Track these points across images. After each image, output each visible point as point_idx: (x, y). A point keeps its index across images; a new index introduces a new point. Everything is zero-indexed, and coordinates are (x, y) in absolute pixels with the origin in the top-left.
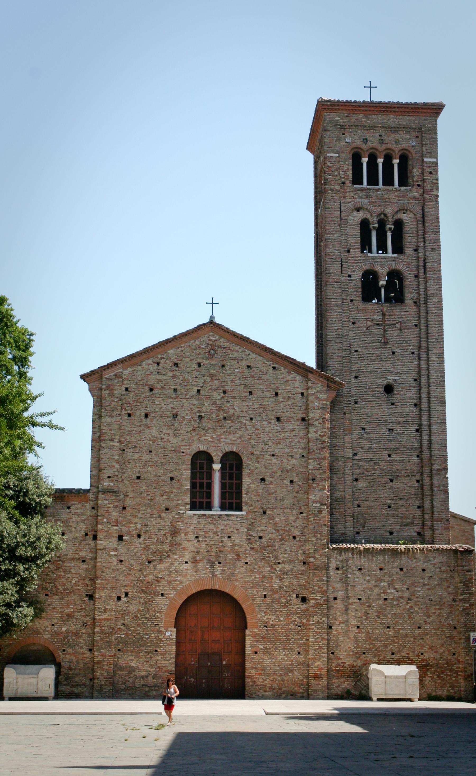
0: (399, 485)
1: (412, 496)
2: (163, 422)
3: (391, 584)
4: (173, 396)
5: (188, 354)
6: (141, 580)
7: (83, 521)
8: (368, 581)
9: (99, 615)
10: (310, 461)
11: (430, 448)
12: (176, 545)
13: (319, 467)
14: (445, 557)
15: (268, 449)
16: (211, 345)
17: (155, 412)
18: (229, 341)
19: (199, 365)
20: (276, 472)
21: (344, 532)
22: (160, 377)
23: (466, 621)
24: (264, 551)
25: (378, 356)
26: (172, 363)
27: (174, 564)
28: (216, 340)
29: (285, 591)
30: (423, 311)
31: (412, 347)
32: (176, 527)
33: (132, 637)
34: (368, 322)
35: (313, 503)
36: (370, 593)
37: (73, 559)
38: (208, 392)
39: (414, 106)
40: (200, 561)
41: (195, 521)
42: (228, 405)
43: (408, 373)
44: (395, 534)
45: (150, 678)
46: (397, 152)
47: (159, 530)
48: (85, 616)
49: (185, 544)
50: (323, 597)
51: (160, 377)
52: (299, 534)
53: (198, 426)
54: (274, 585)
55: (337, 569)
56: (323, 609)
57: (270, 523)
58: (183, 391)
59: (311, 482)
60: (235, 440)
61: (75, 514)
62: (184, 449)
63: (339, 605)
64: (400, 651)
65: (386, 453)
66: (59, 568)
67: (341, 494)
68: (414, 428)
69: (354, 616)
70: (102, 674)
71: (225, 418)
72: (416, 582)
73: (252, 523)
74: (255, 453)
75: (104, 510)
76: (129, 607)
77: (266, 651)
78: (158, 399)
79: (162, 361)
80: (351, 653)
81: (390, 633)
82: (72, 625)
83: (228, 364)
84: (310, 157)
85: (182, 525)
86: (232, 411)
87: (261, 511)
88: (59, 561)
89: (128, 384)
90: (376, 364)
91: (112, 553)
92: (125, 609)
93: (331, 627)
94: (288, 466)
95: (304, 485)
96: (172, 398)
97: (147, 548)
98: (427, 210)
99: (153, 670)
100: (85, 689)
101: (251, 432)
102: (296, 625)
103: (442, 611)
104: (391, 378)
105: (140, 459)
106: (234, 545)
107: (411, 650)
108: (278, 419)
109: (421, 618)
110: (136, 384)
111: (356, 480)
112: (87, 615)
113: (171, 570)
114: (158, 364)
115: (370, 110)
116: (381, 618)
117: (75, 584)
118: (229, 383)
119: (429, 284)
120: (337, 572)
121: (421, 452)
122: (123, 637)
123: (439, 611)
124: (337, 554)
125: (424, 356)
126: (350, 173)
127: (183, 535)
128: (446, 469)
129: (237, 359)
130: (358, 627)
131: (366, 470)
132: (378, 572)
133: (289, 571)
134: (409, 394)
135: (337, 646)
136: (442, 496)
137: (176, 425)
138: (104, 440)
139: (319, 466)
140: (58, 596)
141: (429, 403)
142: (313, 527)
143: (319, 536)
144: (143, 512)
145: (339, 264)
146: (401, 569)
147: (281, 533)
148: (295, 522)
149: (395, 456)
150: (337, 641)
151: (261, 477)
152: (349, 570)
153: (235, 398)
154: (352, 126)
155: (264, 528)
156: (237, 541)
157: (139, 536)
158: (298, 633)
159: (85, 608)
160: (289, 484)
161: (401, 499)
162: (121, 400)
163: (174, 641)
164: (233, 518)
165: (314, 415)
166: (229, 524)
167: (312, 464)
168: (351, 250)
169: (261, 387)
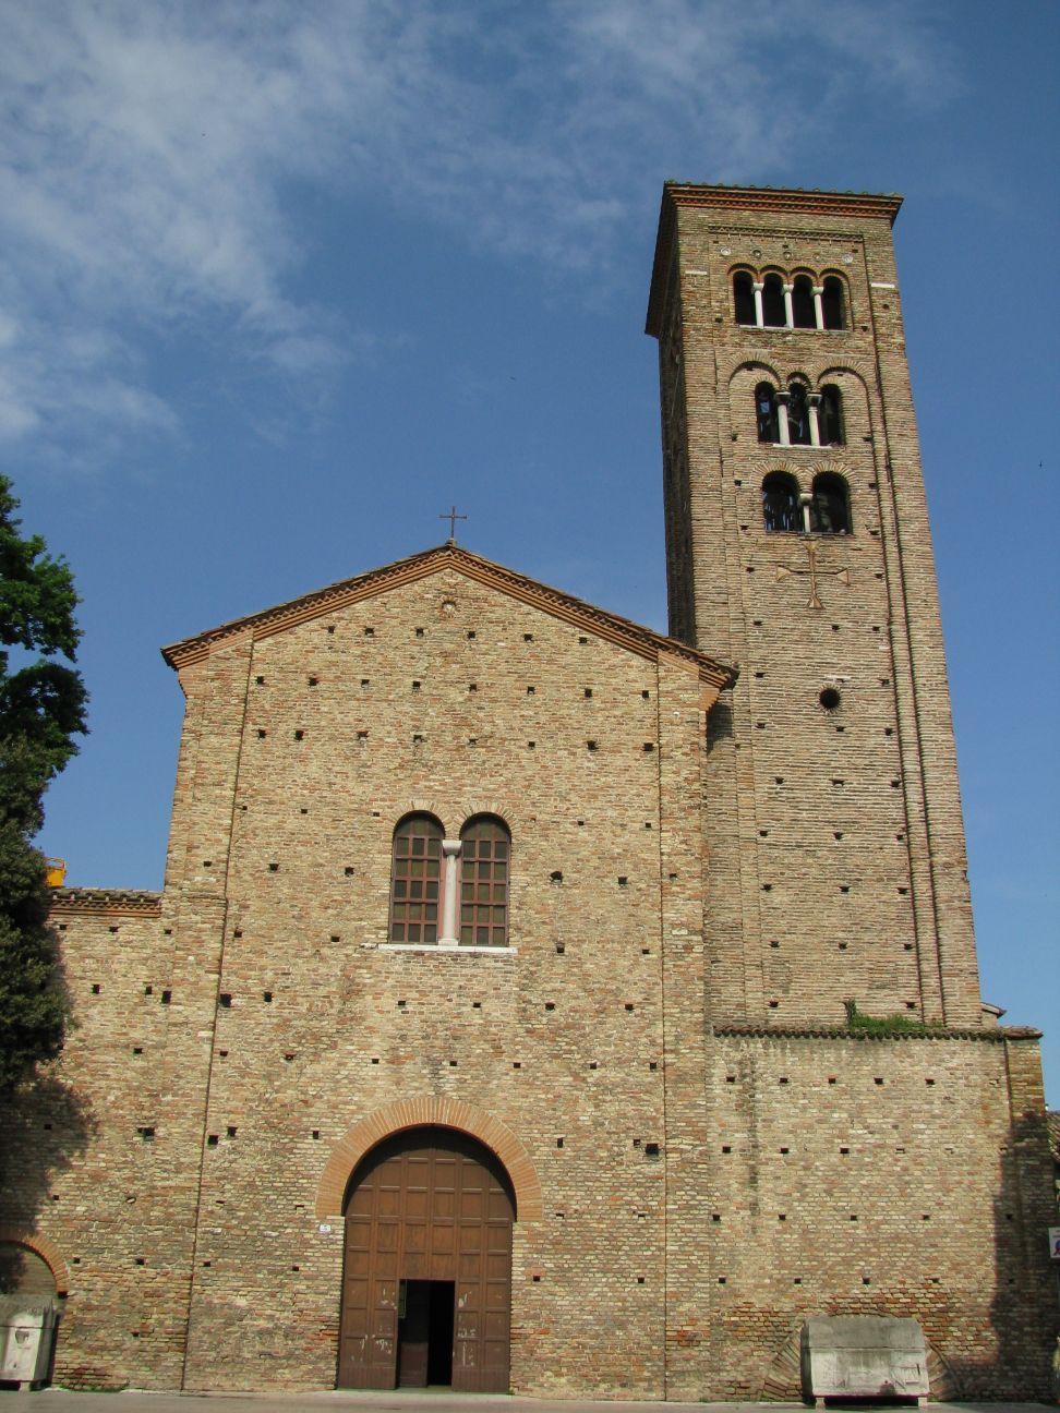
1: (893, 923)
3: (856, 1116)
4: (361, 695)
6: (267, 1100)
8: (804, 1108)
9: (163, 1179)
10: (663, 834)
12: (352, 1019)
16: (446, 593)
17: (319, 728)
19: (420, 631)
20: (588, 861)
23: (1034, 1201)
24: (558, 1039)
25: (807, 634)
27: (345, 1064)
28: (457, 584)
30: (891, 547)
31: (872, 617)
32: (353, 981)
33: (238, 1232)
34: (780, 569)
35: (673, 928)
37: (115, 1046)
42: (481, 715)
45: (278, 1340)
46: (818, 273)
47: (316, 985)
48: (131, 1180)
49: (374, 1019)
52: (639, 998)
54: (581, 1118)
55: (731, 1080)
56: (698, 1173)
57: (574, 975)
58: (381, 684)
60: (494, 790)
64: (881, 1277)
66: (82, 1065)
67: (734, 915)
69: (771, 1191)
70: (161, 1323)
71: (472, 741)
73: (532, 973)
74: (539, 817)
75: (190, 936)
76: (235, 1161)
77: (562, 1276)
78: (326, 702)
79: (339, 626)
80: (767, 1281)
81: (858, 1231)
82: (100, 1199)
84: (653, 343)
85: (369, 976)
86: (488, 728)
87: (553, 946)
88: (81, 1049)
89: (264, 670)
90: (801, 650)
92: (227, 1164)
93: (716, 1218)
95: (652, 890)
97: (284, 1025)
98: (884, 368)
99: (286, 1318)
100: (120, 1358)
101: (530, 773)
103: (976, 1178)
104: (831, 679)
106: (488, 1023)
108: (592, 746)
109: (930, 1194)
112: (136, 1178)
113: (338, 1077)
114: (331, 630)
115: (764, 204)
116: (836, 1195)
117: (114, 1103)
119: (899, 497)
121: (907, 828)
122: (219, 1234)
123: (970, 1178)
125: (900, 635)
126: (731, 305)
127: (369, 998)
129: (502, 622)
130: (782, 1218)
131: (789, 866)
132: (826, 1089)
134: (874, 711)
135: (733, 1262)
137: (364, 755)
138: (202, 785)
140: (74, 1129)
142: (672, 982)
144: (280, 944)
147: (598, 997)
148: (630, 971)
150: (732, 1252)
151: (552, 871)
153: (496, 701)
155: (558, 985)
156: (494, 1014)
157: (268, 997)
158: (638, 1234)
159: (132, 1163)
163: (340, 1246)
166: (476, 976)
168: (739, 437)
169: (554, 678)
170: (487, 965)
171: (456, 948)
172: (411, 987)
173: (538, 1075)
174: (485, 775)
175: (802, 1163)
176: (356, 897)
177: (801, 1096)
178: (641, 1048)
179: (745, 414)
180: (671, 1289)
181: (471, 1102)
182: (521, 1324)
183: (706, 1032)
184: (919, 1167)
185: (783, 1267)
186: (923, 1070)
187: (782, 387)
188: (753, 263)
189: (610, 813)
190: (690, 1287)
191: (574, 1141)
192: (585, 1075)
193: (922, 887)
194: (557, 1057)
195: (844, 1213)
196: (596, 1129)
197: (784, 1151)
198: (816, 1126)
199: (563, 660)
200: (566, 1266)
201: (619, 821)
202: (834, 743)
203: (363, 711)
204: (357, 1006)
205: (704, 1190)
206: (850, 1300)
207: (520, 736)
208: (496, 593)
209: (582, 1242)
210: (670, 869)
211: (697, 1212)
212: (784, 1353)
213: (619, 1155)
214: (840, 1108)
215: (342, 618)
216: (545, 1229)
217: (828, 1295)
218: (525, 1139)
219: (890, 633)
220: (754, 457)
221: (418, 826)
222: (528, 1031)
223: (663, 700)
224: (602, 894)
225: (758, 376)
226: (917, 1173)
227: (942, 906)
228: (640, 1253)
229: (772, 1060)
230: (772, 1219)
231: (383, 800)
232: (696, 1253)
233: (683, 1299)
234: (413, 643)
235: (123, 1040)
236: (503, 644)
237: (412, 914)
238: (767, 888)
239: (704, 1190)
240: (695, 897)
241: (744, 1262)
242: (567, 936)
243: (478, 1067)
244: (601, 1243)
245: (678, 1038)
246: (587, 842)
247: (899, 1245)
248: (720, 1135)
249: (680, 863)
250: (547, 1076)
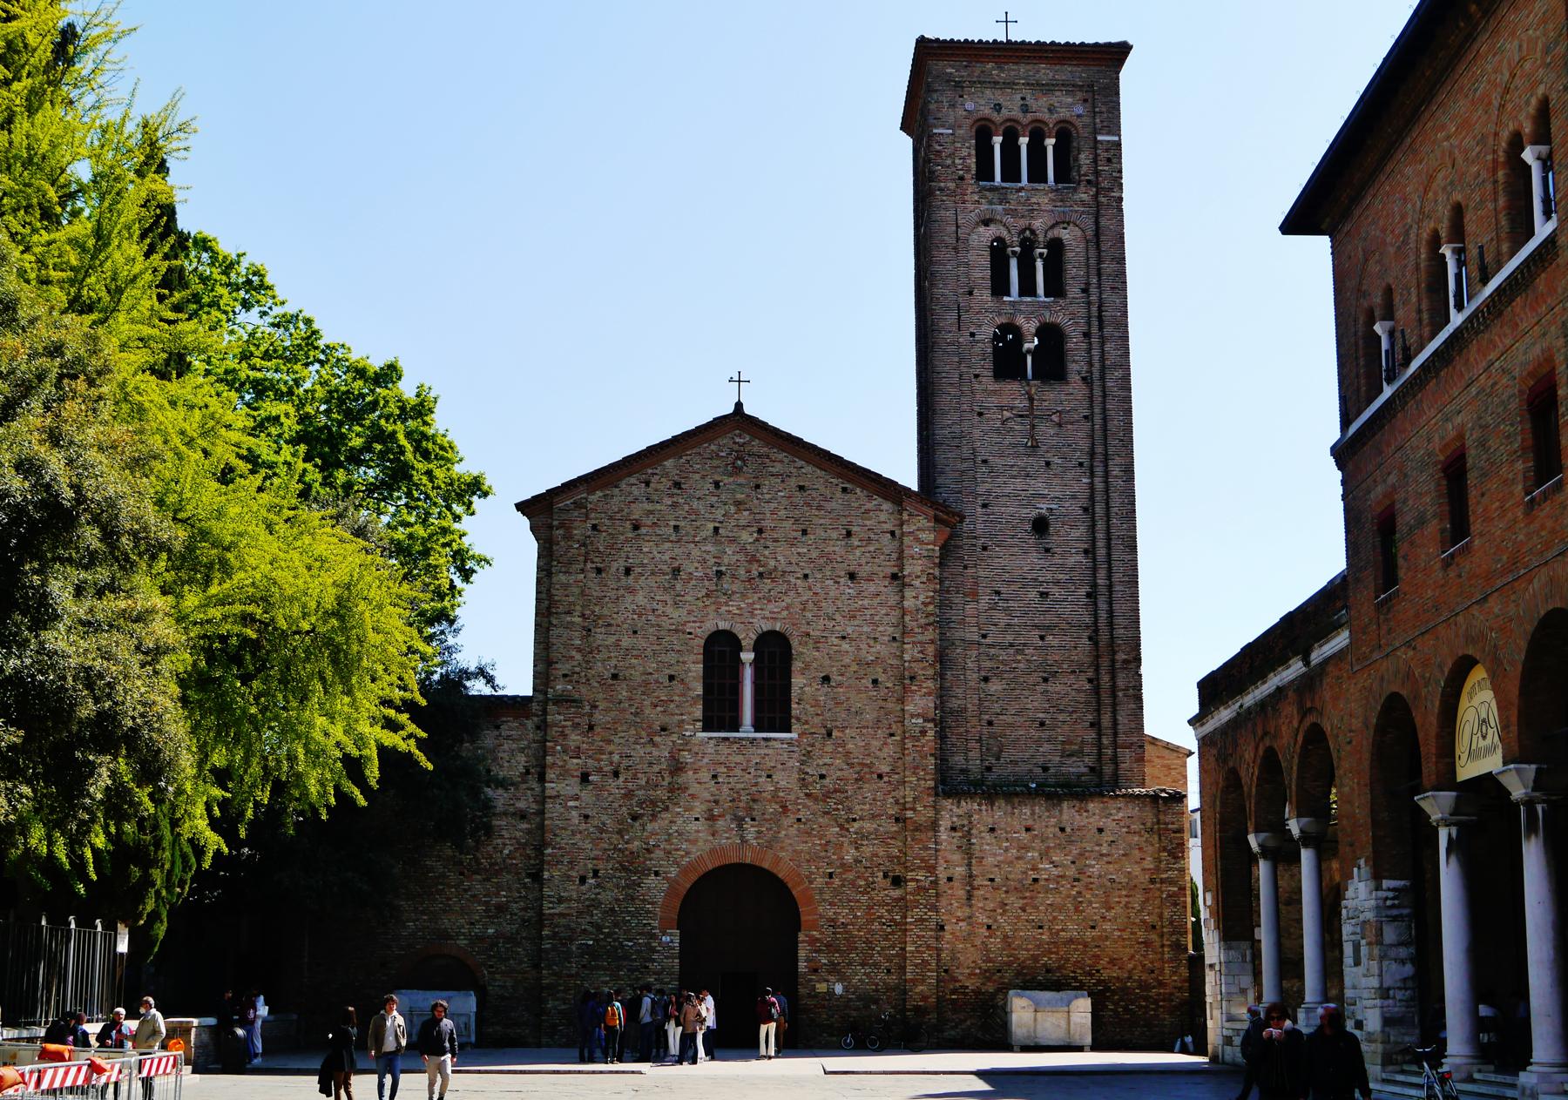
0: (1059, 688)
3: (1045, 855)
4: (673, 538)
7: (522, 750)
8: (1006, 850)
11: (1111, 625)
17: (643, 565)
18: (768, 445)
19: (717, 484)
22: (650, 507)
30: (1097, 392)
37: (505, 814)
41: (710, 748)
43: (1074, 497)
48: (525, 909)
49: (694, 789)
51: (650, 507)
52: (887, 769)
55: (953, 829)
61: (508, 737)
68: (1083, 591)
71: (761, 575)
77: (834, 969)
79: (654, 479)
84: (908, 142)
86: (772, 563)
90: (1019, 483)
91: (571, 804)
93: (942, 928)
97: (629, 795)
98: (1103, 222)
104: (1043, 507)
105: (617, 645)
106: (777, 789)
110: (611, 518)
111: (986, 679)
114: (647, 484)
119: (1108, 347)
121: (1096, 631)
125: (1099, 470)
128: (1138, 660)
130: (989, 927)
134: (1076, 534)
137: (679, 587)
141: (1109, 547)
145: (955, 314)
146: (1062, 830)
155: (828, 761)
157: (616, 774)
158: (886, 939)
161: (1062, 711)
162: (584, 545)
165: (913, 568)
193: (1105, 679)
197: (992, 880)
199: (829, 506)
204: (681, 779)
219: (1092, 467)
224: (859, 692)
225: (992, 231)
229: (983, 814)
235: (512, 809)
237: (719, 712)
239: (935, 908)
240: (929, 694)
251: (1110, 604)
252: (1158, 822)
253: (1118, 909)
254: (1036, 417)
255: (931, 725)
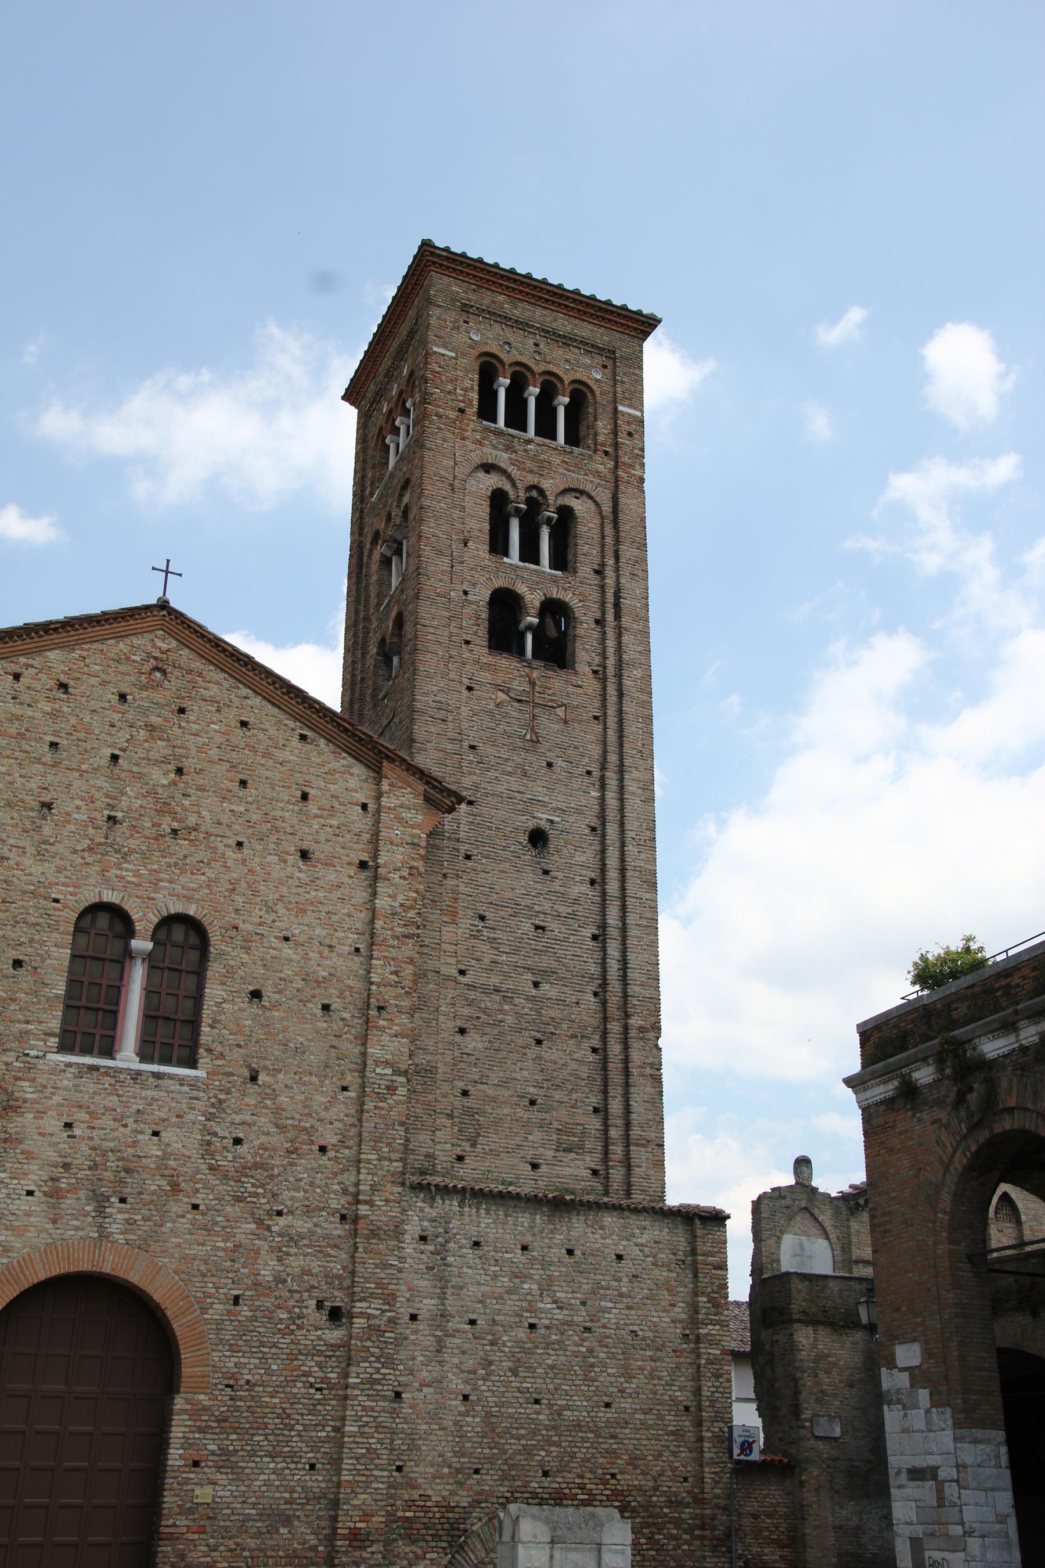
0: (555, 1055)
1: (583, 1083)
2: (12, 818)
3: (546, 1287)
5: (98, 667)
8: (495, 1277)
11: (624, 979)
13: (396, 979)
14: (667, 1230)
15: (274, 921)
16: (156, 658)
19: (123, 697)
21: (431, 1151)
22: (17, 710)
23: (713, 1392)
24: (243, 1179)
26: (52, 683)
28: (169, 650)
29: (290, 1291)
30: (611, 690)
34: (500, 693)
35: (377, 1066)
36: (497, 1307)
38: (138, 765)
39: (604, 306)
40: (68, 1191)
42: (186, 803)
44: (544, 1169)
46: (566, 382)
50: (384, 1311)
51: (17, 710)
52: (334, 1140)
53: (103, 840)
54: (262, 1272)
55: (423, 1239)
56: (385, 1342)
59: (373, 1013)
60: (194, 890)
62: (60, 892)
63: (423, 1335)
64: (563, 1468)
65: (529, 976)
67: (429, 1058)
71: (175, 832)
72: (602, 1288)
73: (221, 1101)
74: (241, 926)
77: (226, 1460)
80: (446, 1470)
81: (541, 1417)
83: (195, 710)
85: (31, 1090)
86: (192, 820)
87: (247, 1073)
93: (398, 1395)
94: (319, 968)
95: (356, 1021)
96: (45, 764)
98: (623, 500)
101: (235, 875)
102: (311, 1386)
103: (658, 1364)
104: (542, 818)
106: (166, 1156)
107: (588, 1465)
108: (304, 855)
109: (613, 1379)
114: (17, 677)
115: (521, 291)
116: (521, 1374)
118: (193, 751)
119: (625, 639)
120: (422, 1247)
121: (604, 984)
123: (653, 1364)
124: (424, 1201)
125: (612, 782)
128: (657, 1028)
129: (217, 702)
130: (466, 1398)
132: (518, 1256)
133: (302, 1237)
134: (580, 858)
135: (413, 1447)
136: (649, 1089)
137: (47, 830)
139: (394, 977)
143: (386, 1150)
145: (447, 560)
146: (570, 1252)
148: (326, 1109)
149: (547, 987)
151: (251, 988)
152: (451, 1245)
153: (204, 790)
154: (483, 310)
155: (248, 1118)
160: (319, 1012)
164: (171, 1082)
165: (391, 857)
166: (157, 1100)
167: (380, 971)
168: (470, 544)
169: (268, 774)
170: (172, 1088)
171: (137, 1065)
172: (81, 1107)
173: (219, 1219)
174: (186, 872)
175: (489, 1337)
176: (24, 996)
177: (492, 1262)
178: (332, 1196)
179: (479, 521)
180: (347, 1478)
181: (139, 1248)
182: (171, 1521)
183: (403, 1184)
184: (605, 1350)
185: (463, 1455)
186: (614, 1244)
187: (518, 499)
188: (502, 356)
189: (318, 931)
190: (367, 1476)
191: (252, 1298)
192: (269, 1223)
193: (615, 1049)
194: (239, 1199)
195: (528, 1395)
196: (277, 1286)
197: (472, 1322)
198: (506, 1296)
199: (280, 755)
200: (231, 1448)
201: (327, 941)
202: (538, 886)
203: (50, 778)
205: (389, 1362)
206: (528, 1495)
207: (228, 833)
208: (212, 668)
209: (251, 1419)
210: (378, 1000)
211: (380, 1387)
212: (457, 1556)
213: (299, 1318)
214: (531, 1279)
215: (32, 666)
216: (212, 1403)
217: (506, 1489)
218: (198, 1294)
220: (483, 568)
221: (104, 923)
222: (211, 1168)
223: (384, 816)
224: (303, 1020)
226: (602, 1355)
227: (634, 1071)
228: (314, 1434)
230: (455, 1399)
231: (65, 885)
232: (376, 1435)
233: (358, 1490)
234: (112, 708)
236: (217, 727)
237: (88, 1027)
238: (462, 1031)
239: (389, 1362)
241: (423, 1448)
242: (262, 1063)
243: (151, 1207)
244: (272, 1422)
245: (374, 1188)
246: (291, 960)
247: (580, 1434)
248: (408, 1300)
249: (389, 995)
250: (228, 1221)
251: (624, 951)
252: (693, 1252)
253: (639, 1381)
254: (536, 705)
255: (403, 1080)
